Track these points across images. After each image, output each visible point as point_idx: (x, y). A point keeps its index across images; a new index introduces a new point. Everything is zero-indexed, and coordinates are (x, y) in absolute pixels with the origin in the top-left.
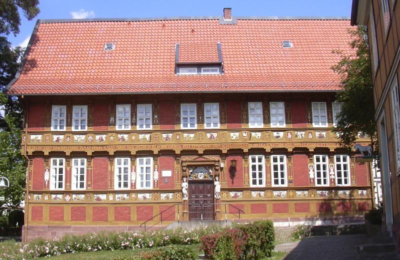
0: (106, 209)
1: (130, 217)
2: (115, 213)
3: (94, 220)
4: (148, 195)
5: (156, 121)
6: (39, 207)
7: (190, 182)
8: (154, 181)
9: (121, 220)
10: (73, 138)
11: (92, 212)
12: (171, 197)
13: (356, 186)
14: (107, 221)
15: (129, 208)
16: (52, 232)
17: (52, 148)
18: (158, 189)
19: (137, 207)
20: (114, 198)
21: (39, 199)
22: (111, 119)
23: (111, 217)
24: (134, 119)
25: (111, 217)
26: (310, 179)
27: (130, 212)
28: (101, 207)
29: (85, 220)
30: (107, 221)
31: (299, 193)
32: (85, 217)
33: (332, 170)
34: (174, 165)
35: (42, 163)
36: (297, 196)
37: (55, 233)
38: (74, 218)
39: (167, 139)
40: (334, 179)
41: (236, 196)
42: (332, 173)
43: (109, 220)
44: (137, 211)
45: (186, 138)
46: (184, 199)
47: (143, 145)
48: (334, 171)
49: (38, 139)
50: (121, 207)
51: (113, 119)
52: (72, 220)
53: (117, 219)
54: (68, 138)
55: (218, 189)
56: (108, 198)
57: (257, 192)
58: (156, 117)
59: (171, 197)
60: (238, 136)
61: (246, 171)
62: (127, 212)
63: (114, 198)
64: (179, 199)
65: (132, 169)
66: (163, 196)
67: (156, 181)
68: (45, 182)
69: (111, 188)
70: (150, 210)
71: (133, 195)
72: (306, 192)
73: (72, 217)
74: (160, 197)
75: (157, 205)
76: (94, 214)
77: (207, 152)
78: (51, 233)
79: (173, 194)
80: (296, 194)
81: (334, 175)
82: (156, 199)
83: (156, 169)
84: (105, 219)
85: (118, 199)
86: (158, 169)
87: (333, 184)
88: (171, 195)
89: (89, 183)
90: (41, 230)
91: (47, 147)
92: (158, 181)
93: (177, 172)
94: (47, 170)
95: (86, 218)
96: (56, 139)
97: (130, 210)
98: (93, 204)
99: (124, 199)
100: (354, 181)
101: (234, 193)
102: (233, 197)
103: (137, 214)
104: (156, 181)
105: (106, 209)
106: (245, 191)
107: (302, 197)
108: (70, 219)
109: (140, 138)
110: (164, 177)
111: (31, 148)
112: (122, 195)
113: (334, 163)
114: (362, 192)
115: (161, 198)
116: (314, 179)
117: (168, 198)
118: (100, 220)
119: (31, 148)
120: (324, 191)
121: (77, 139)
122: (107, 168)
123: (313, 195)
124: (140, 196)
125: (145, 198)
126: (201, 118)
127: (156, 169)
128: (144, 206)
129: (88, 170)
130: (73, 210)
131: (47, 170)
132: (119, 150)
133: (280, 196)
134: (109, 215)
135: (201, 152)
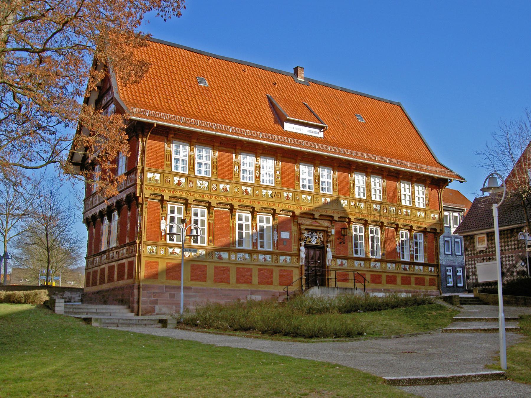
0: (228, 269)
1: (251, 280)
2: (237, 275)
3: (215, 281)
4: (268, 257)
5: (278, 178)
6: (153, 262)
7: (306, 247)
8: (274, 242)
9: (243, 283)
10: (196, 183)
11: (213, 271)
12: (288, 261)
13: (427, 262)
14: (229, 283)
15: (250, 270)
16: (170, 294)
17: (173, 192)
18: (277, 251)
19: (259, 269)
20: (236, 257)
21: (153, 252)
22: (235, 168)
23: (233, 279)
24: (257, 172)
25: (233, 279)
26: (397, 253)
27: (251, 274)
29: (206, 282)
30: (229, 283)
31: (389, 265)
32: (206, 277)
33: (412, 246)
35: (158, 209)
36: (388, 268)
37: (174, 294)
39: (287, 199)
40: (413, 255)
41: (342, 265)
43: (231, 282)
44: (259, 274)
46: (301, 264)
47: (267, 202)
48: (413, 248)
49: (156, 178)
50: (243, 268)
51: (238, 168)
52: (192, 280)
53: (238, 281)
54: (191, 183)
55: (329, 255)
56: (229, 258)
57: (358, 261)
58: (278, 173)
59: (288, 261)
60: (346, 204)
61: (350, 240)
62: (249, 274)
63: (236, 257)
64: (296, 264)
65: (253, 227)
66: (282, 258)
67: (275, 242)
68: (161, 232)
69: (233, 246)
70: (270, 273)
71: (255, 256)
72: (394, 265)
73: (191, 276)
74: (280, 260)
75: (277, 269)
76: (216, 275)
77: (323, 217)
78: (168, 295)
79: (290, 257)
80: (386, 266)
81: (413, 251)
82: (276, 262)
83: (276, 230)
84: (226, 280)
85: (240, 259)
86: (277, 229)
87: (412, 260)
88: (288, 258)
89: (211, 238)
90: (157, 291)
91: (167, 190)
92: (277, 242)
94: (164, 218)
95: (207, 279)
96: (177, 182)
97: (251, 272)
98: (215, 262)
99: (246, 259)
100: (426, 259)
101: (340, 260)
102: (340, 265)
104: (275, 242)
105: (228, 269)
106: (349, 260)
107: (391, 270)
108: (190, 279)
109: (263, 194)
110: (283, 238)
111: (149, 189)
112: (243, 254)
113: (413, 240)
114: (431, 269)
116: (399, 253)
117: (285, 261)
118: (221, 282)
119: (149, 189)
120: (406, 266)
121: (199, 185)
122: (229, 222)
123: (399, 269)
124: (261, 257)
126: (317, 181)
127: (276, 230)
128: (265, 269)
129: (209, 224)
130: (194, 269)
131: (164, 218)
132: (243, 204)
133: (375, 267)
134: (231, 275)
135: (317, 216)
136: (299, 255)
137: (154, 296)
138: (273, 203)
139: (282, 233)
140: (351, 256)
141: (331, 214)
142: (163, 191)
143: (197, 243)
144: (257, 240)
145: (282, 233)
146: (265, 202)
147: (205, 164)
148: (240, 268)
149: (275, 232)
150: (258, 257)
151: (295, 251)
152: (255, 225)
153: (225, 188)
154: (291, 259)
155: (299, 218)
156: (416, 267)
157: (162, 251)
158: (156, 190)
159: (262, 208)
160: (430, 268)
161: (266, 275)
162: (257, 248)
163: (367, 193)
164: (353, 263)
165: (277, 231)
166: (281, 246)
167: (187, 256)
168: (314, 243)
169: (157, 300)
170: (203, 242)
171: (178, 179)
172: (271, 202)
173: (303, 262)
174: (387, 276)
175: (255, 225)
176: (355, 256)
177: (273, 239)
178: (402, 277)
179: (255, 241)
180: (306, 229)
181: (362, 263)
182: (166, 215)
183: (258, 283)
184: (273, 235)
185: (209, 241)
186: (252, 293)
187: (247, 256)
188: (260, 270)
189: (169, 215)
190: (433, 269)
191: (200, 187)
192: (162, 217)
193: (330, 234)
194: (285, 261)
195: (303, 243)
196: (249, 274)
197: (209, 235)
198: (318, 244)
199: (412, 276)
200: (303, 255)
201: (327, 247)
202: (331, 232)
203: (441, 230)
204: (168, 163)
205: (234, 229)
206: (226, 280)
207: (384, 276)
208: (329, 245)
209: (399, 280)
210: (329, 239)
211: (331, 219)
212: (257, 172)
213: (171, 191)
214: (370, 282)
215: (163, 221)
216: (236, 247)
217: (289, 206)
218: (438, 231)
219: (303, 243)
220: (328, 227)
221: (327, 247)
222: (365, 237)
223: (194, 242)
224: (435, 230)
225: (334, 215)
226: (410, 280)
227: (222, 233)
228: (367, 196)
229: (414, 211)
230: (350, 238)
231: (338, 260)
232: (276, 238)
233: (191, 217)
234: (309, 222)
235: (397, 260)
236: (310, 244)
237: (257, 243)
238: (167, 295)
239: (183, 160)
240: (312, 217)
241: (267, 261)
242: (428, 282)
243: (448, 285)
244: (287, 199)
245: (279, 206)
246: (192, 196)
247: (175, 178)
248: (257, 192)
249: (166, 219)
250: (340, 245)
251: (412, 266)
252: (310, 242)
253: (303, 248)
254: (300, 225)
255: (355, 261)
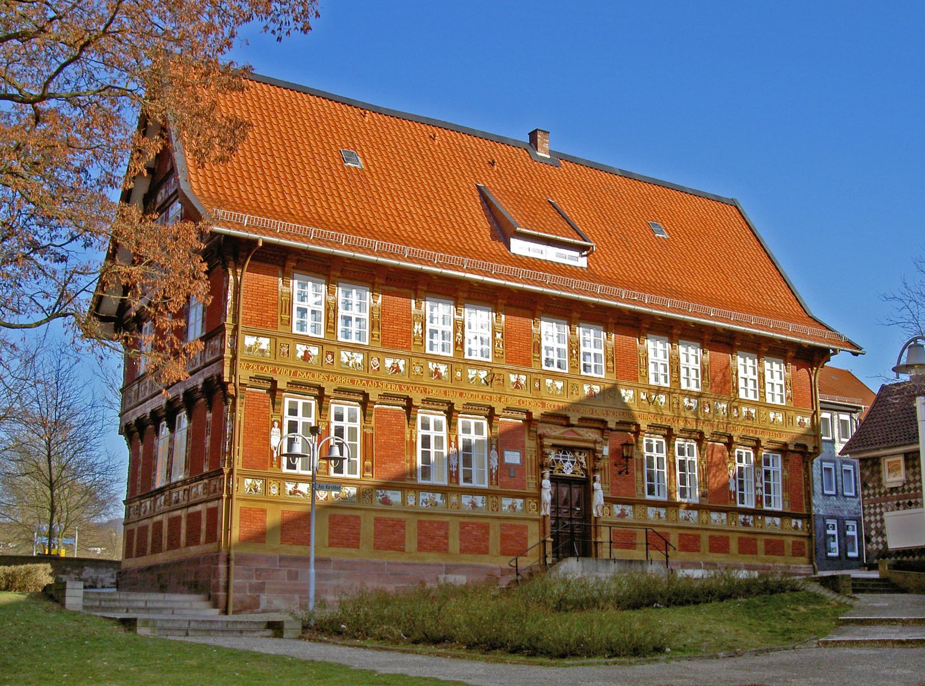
0: (401, 524)
1: (447, 544)
2: (419, 535)
3: (377, 547)
4: (479, 500)
5: (499, 346)
6: (256, 510)
7: (553, 479)
8: (490, 471)
9: (430, 551)
10: (339, 356)
11: (373, 528)
12: (519, 507)
13: (788, 511)
14: (403, 550)
15: (444, 525)
16: (289, 572)
17: (295, 374)
18: (498, 488)
19: (461, 523)
21: (256, 490)
22: (416, 326)
23: (411, 543)
24: (459, 334)
25: (411, 543)
26: (731, 492)
27: (447, 533)
28: (393, 520)
29: (358, 548)
30: (403, 550)
31: (714, 516)
32: (358, 540)
33: (759, 479)
34: (524, 442)
35: (265, 407)
36: (712, 522)
37: (297, 573)
38: (335, 541)
39: (517, 387)
40: (761, 496)
41: (623, 515)
42: (758, 484)
43: (407, 550)
44: (461, 533)
45: (549, 388)
46: (543, 513)
48: (761, 482)
49: (262, 347)
50: (431, 522)
51: (420, 327)
52: (331, 545)
53: (421, 547)
54: (330, 356)
55: (598, 497)
58: (499, 336)
59: (519, 507)
60: (632, 396)
61: (639, 467)
62: (442, 532)
64: (533, 513)
65: (450, 441)
66: (506, 502)
67: (494, 471)
68: (272, 452)
69: (412, 479)
70: (484, 531)
71: (454, 498)
72: (724, 516)
73: (330, 537)
76: (378, 534)
77: (586, 422)
78: (286, 573)
79: (522, 501)
80: (710, 518)
81: (761, 488)
82: (495, 509)
83: (494, 446)
84: (397, 546)
85: (424, 505)
87: (759, 505)
88: (519, 502)
89: (368, 463)
91: (283, 369)
92: (497, 471)
93: (529, 457)
94: (276, 424)
95: (361, 542)
97: (447, 529)
98: (375, 510)
99: (436, 504)
100: (786, 503)
101: (620, 506)
102: (619, 516)
103: (460, 540)
104: (494, 471)
105: (401, 524)
106: (638, 507)
107: (718, 525)
108: (327, 542)
109: (470, 377)
111: (248, 367)
112: (431, 494)
113: (761, 467)
114: (797, 523)
115: (503, 508)
116: (735, 493)
117: (513, 507)
118: (388, 548)
119: (248, 367)
120: (747, 517)
121: (345, 360)
122: (403, 433)
123: (733, 523)
124: (466, 500)
125: (474, 505)
126: (574, 352)
127: (494, 446)
128: (473, 524)
129: (365, 435)
131: (276, 424)
132: (431, 396)
133: (688, 520)
134: (407, 536)
135: (574, 421)
136: (539, 497)
137: (258, 578)
138: (489, 395)
139: (506, 453)
140: (642, 498)
141: (602, 417)
142: (274, 371)
143: (342, 472)
144: (458, 467)
145: (506, 453)
146: (474, 393)
147: (358, 320)
148: (425, 522)
149: (494, 452)
150: (460, 500)
151: (531, 489)
152: (453, 439)
153: (396, 366)
154: (524, 505)
155: (540, 425)
156: (768, 520)
157: (274, 487)
158: (262, 369)
159: (468, 404)
160: (794, 522)
161: (476, 536)
162: (458, 483)
163: (671, 377)
164: (645, 512)
165: (497, 450)
166: (505, 480)
167: (321, 499)
168: (568, 473)
169: (264, 583)
170: (352, 470)
171: (304, 348)
172: (485, 394)
173: (547, 511)
174: (710, 537)
175: (453, 439)
176: (648, 497)
177: (489, 465)
178: (740, 539)
179: (454, 469)
180: (554, 446)
181: (663, 511)
182: (282, 418)
183: (461, 550)
184: (489, 458)
185: (365, 469)
186: (449, 570)
187: (438, 497)
188: (463, 525)
189: (287, 418)
190: (800, 523)
191: (347, 364)
192: (273, 422)
193: (600, 456)
194: (513, 507)
195: (547, 473)
196: (442, 532)
197: (364, 458)
198: (577, 476)
199: (759, 537)
200: (547, 496)
201: (594, 480)
202: (601, 452)
203: (815, 448)
204: (286, 317)
205: (413, 445)
206: (397, 546)
207: (705, 537)
208: (598, 476)
209: (734, 545)
210: (599, 465)
211: (601, 426)
212: (459, 334)
213: (290, 372)
214: (677, 548)
215: (276, 430)
216: (416, 480)
217: (519, 401)
218: (810, 450)
219: (547, 473)
220: (595, 442)
221: (594, 480)
222: (668, 461)
223: (335, 472)
224: (805, 447)
225: (607, 419)
226: (755, 546)
227: (390, 452)
228: (672, 382)
229: (763, 411)
230: (639, 463)
231: (615, 506)
232: (495, 464)
233: (329, 423)
234: (559, 431)
235: (731, 505)
236: (561, 474)
237: (457, 472)
238: (284, 573)
239: (313, 312)
240: (564, 423)
241: (477, 507)
242: (790, 550)
243: (829, 554)
244: (517, 387)
245: (500, 400)
246: (332, 380)
247: (298, 347)
248: (459, 374)
249: (281, 426)
250: (619, 476)
251: (760, 518)
252: (561, 470)
253: (546, 483)
254: (541, 437)
255: (649, 508)
